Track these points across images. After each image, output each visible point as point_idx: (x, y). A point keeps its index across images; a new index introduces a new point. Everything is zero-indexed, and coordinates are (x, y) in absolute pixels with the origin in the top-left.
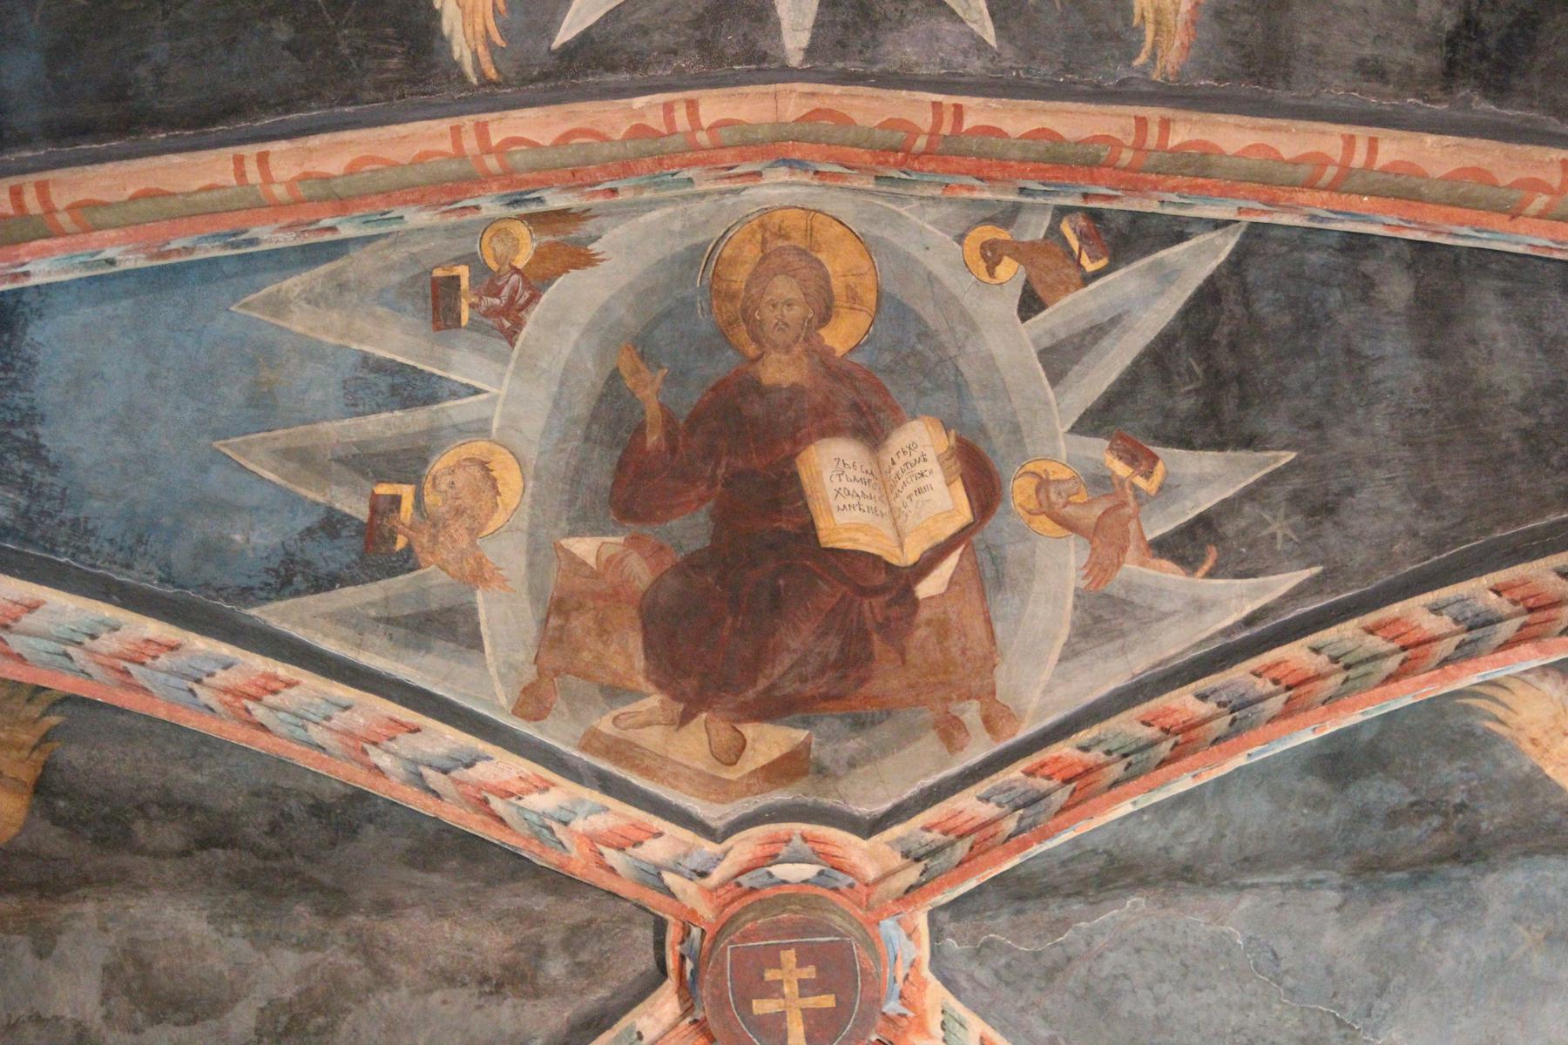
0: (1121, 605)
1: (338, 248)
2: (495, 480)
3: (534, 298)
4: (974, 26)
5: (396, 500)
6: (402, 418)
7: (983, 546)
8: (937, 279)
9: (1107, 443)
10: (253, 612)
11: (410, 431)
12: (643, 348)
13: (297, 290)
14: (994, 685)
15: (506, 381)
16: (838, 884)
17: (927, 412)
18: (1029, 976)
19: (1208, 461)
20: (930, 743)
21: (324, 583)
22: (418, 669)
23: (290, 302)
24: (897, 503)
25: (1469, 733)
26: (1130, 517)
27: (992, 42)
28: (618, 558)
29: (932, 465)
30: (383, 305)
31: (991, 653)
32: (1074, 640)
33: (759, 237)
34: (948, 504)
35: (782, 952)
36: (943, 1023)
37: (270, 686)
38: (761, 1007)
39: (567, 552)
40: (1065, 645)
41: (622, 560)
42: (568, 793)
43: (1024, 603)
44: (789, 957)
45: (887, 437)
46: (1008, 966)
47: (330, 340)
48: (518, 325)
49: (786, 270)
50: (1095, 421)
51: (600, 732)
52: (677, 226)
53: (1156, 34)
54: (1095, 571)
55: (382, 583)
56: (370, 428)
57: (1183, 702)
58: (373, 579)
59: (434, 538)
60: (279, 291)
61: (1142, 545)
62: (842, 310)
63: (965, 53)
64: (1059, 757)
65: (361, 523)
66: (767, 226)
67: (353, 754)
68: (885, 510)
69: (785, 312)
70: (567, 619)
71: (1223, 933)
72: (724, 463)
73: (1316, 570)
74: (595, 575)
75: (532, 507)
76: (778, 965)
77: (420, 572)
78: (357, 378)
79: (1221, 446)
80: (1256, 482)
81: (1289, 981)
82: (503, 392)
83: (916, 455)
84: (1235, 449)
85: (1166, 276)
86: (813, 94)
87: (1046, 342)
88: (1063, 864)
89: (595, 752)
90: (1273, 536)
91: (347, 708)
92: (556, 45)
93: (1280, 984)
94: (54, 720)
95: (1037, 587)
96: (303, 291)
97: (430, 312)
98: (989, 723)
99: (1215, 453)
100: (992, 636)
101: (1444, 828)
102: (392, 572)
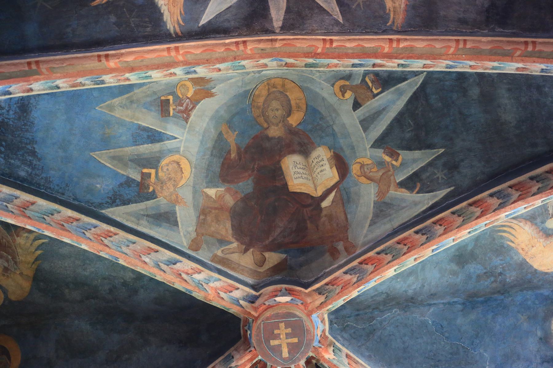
0: (388, 205)
1: (130, 87)
2: (181, 168)
3: (194, 107)
4: (335, 17)
5: (149, 175)
6: (151, 146)
8: (326, 99)
9: (383, 150)
10: (103, 211)
11: (154, 151)
12: (230, 124)
13: (117, 103)
14: (348, 236)
15: (185, 135)
16: (298, 303)
17: (324, 144)
18: (362, 336)
19: (417, 154)
20: (327, 257)
22: (157, 232)
23: (115, 107)
24: (314, 176)
25: (502, 246)
26: (391, 175)
27: (341, 21)
28: (222, 196)
29: (326, 162)
30: (145, 108)
31: (347, 225)
32: (374, 218)
33: (267, 88)
34: (331, 175)
36: (333, 350)
37: (109, 235)
38: (273, 343)
39: (206, 193)
40: (371, 220)
41: (224, 196)
43: (357, 207)
44: (282, 325)
45: (310, 153)
46: (354, 333)
47: (127, 119)
48: (189, 116)
49: (276, 99)
50: (379, 143)
51: (217, 255)
52: (240, 84)
53: (394, 15)
54: (380, 194)
55: (145, 202)
56: (141, 150)
58: (142, 201)
59: (162, 187)
60: (111, 103)
61: (395, 184)
62: (294, 111)
63: (333, 25)
64: (370, 257)
65: (138, 182)
66: (269, 83)
67: (137, 257)
68: (310, 178)
69: (276, 112)
70: (206, 216)
71: (425, 320)
72: (257, 164)
73: (452, 188)
74: (215, 201)
75: (194, 178)
76: (278, 328)
77: (157, 199)
78: (137, 133)
79: (420, 149)
80: (432, 160)
81: (447, 335)
82: (184, 138)
83: (320, 159)
84: (425, 149)
85: (400, 93)
86: (284, 39)
87: (362, 118)
88: (372, 297)
89: (216, 262)
90: (438, 178)
91: (134, 243)
92: (201, 24)
93: (443, 336)
94: (39, 252)
95: (361, 201)
96: (119, 103)
97: (160, 111)
98: (346, 249)
99: (418, 151)
100: (347, 219)
101: (495, 281)
102: (148, 199)
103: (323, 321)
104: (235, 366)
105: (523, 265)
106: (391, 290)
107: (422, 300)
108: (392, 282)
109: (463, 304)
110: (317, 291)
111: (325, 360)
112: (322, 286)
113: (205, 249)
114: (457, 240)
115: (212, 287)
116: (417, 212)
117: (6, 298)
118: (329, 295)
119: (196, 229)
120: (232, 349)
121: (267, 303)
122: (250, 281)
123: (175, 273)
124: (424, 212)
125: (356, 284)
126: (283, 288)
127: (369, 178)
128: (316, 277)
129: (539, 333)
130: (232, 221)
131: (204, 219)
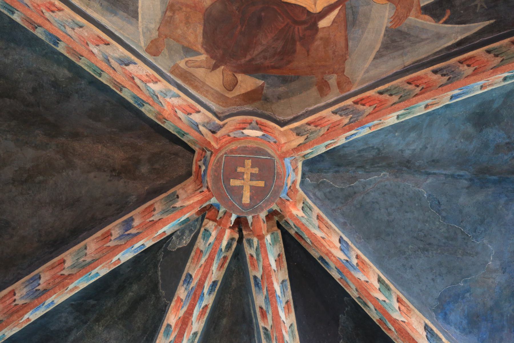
0: (404, 35)
7: (349, 7)
14: (344, 68)
16: (270, 141)
18: (337, 197)
20: (314, 92)
31: (346, 54)
32: (381, 50)
35: (246, 160)
36: (303, 207)
40: (377, 52)
42: (165, 86)
43: (363, 32)
44: (248, 163)
46: (330, 192)
54: (396, 20)
61: (418, 9)
64: (370, 96)
67: (83, 44)
70: (174, 13)
71: (419, 191)
73: (492, 21)
76: (243, 166)
81: (444, 214)
88: (359, 151)
90: (476, 6)
91: (81, 27)
93: (440, 214)
95: (370, 26)
98: (339, 85)
100: (347, 46)
103: (295, 170)
104: (179, 206)
106: (384, 146)
107: (419, 165)
108: (389, 136)
109: (471, 180)
110: (296, 131)
111: (292, 216)
112: (302, 125)
113: (166, 55)
114: (487, 88)
115: (168, 103)
116: (439, 47)
118: (310, 136)
119: (159, 28)
120: (179, 186)
121: (232, 135)
123: (127, 74)
124: (448, 48)
125: (347, 126)
126: (253, 120)
128: (295, 115)
130: (205, 26)
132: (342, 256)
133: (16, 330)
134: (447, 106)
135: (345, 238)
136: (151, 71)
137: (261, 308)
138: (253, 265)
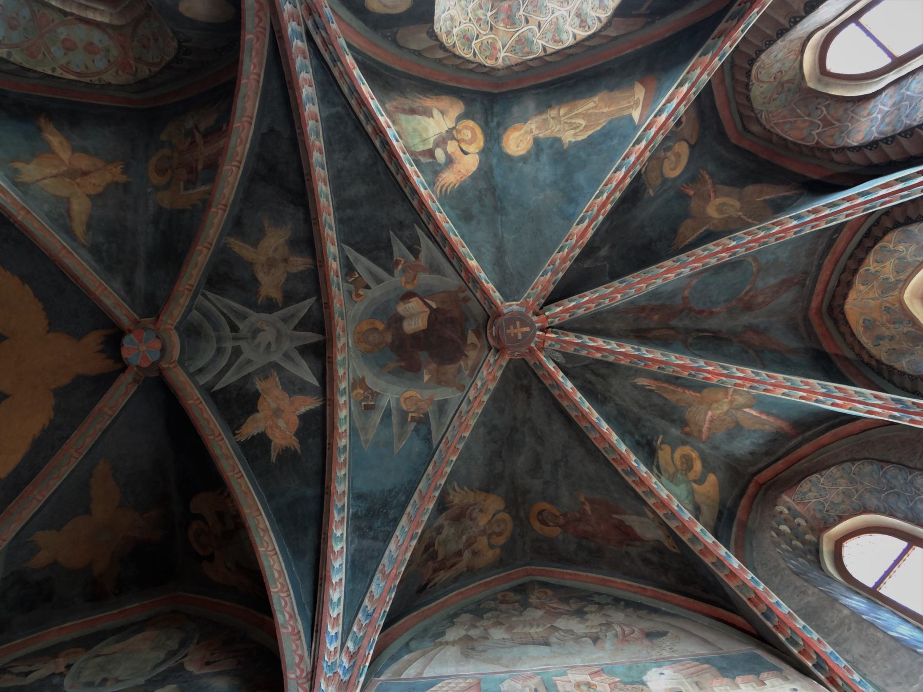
3: (371, 389)
5: (412, 417)
19: (395, 248)
21: (430, 432)
38: (520, 337)
39: (427, 381)
47: (375, 431)
48: (376, 392)
50: (391, 273)
57: (446, 250)
59: (422, 409)
66: (357, 342)
87: (376, 284)
94: (466, 488)
101: (486, 195)
102: (428, 418)
103: (510, 306)
105: (474, 177)
109: (502, 215)
117: (504, 511)
122: (486, 352)
124: (433, 242)
127: (415, 278)
129: (521, 164)
131: (444, 382)
132: (549, 274)
133: (614, 434)
134: (462, 237)
135: (541, 274)
136: (472, 388)
137: (585, 310)
138: (563, 319)
